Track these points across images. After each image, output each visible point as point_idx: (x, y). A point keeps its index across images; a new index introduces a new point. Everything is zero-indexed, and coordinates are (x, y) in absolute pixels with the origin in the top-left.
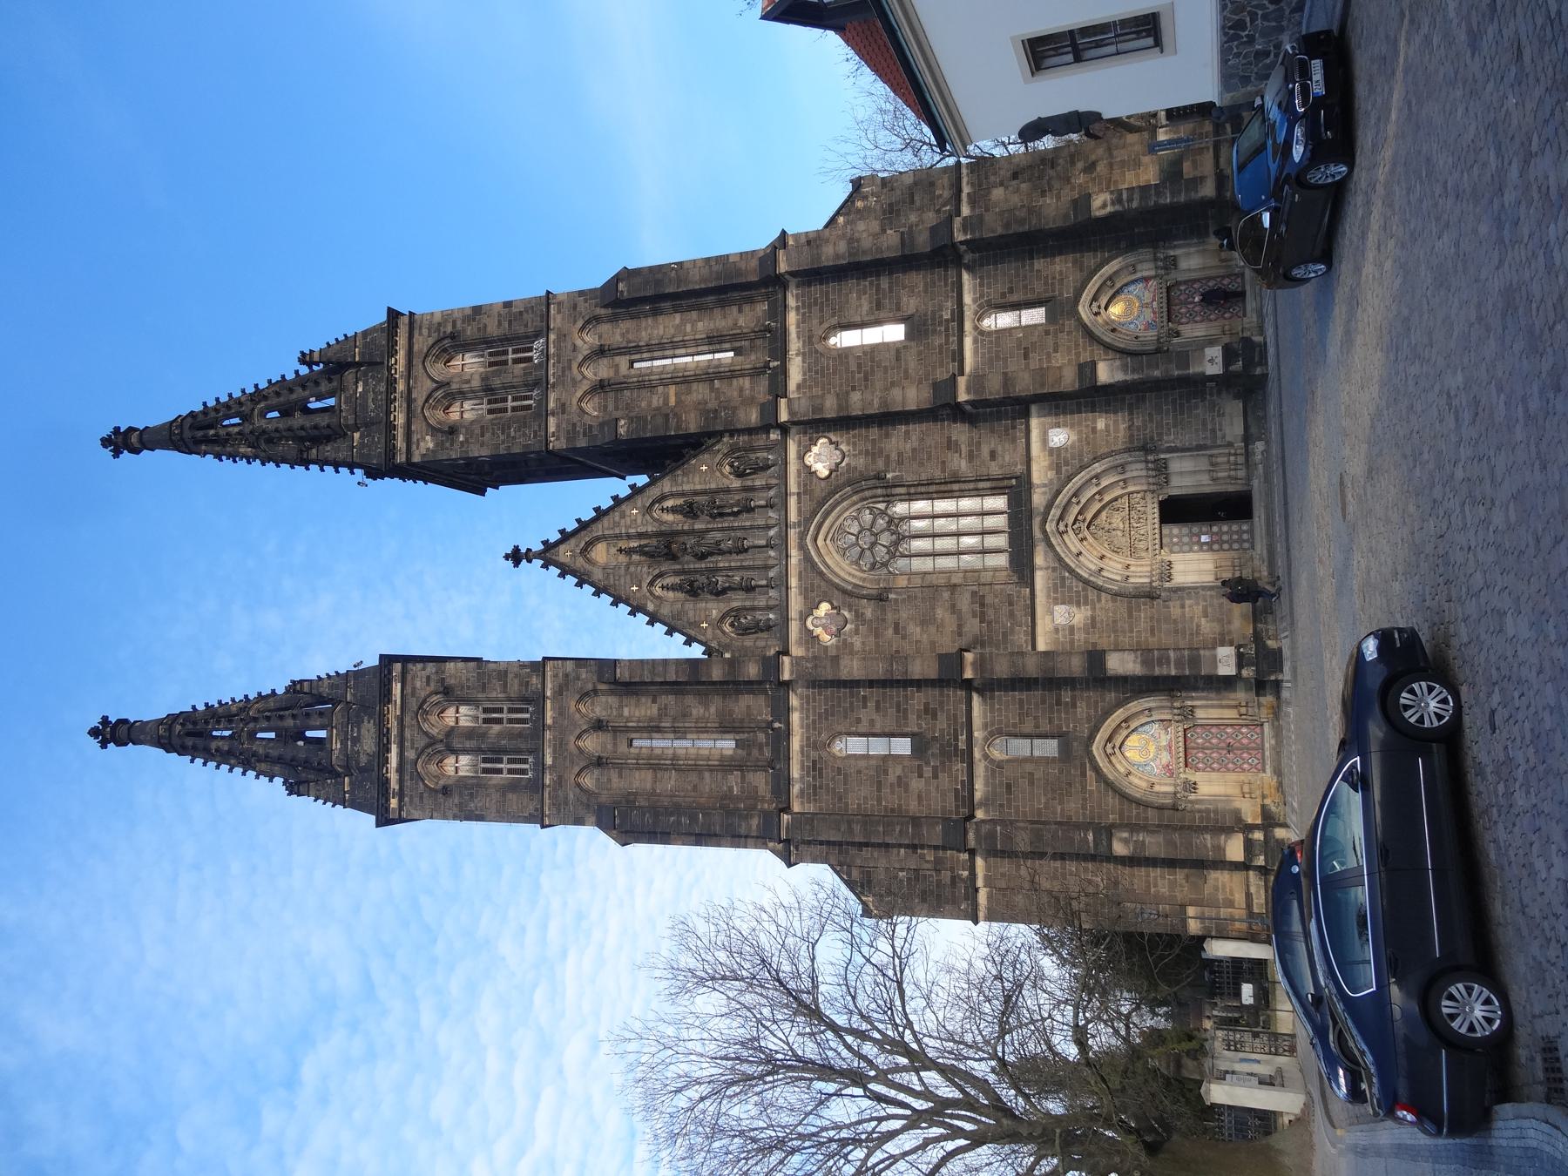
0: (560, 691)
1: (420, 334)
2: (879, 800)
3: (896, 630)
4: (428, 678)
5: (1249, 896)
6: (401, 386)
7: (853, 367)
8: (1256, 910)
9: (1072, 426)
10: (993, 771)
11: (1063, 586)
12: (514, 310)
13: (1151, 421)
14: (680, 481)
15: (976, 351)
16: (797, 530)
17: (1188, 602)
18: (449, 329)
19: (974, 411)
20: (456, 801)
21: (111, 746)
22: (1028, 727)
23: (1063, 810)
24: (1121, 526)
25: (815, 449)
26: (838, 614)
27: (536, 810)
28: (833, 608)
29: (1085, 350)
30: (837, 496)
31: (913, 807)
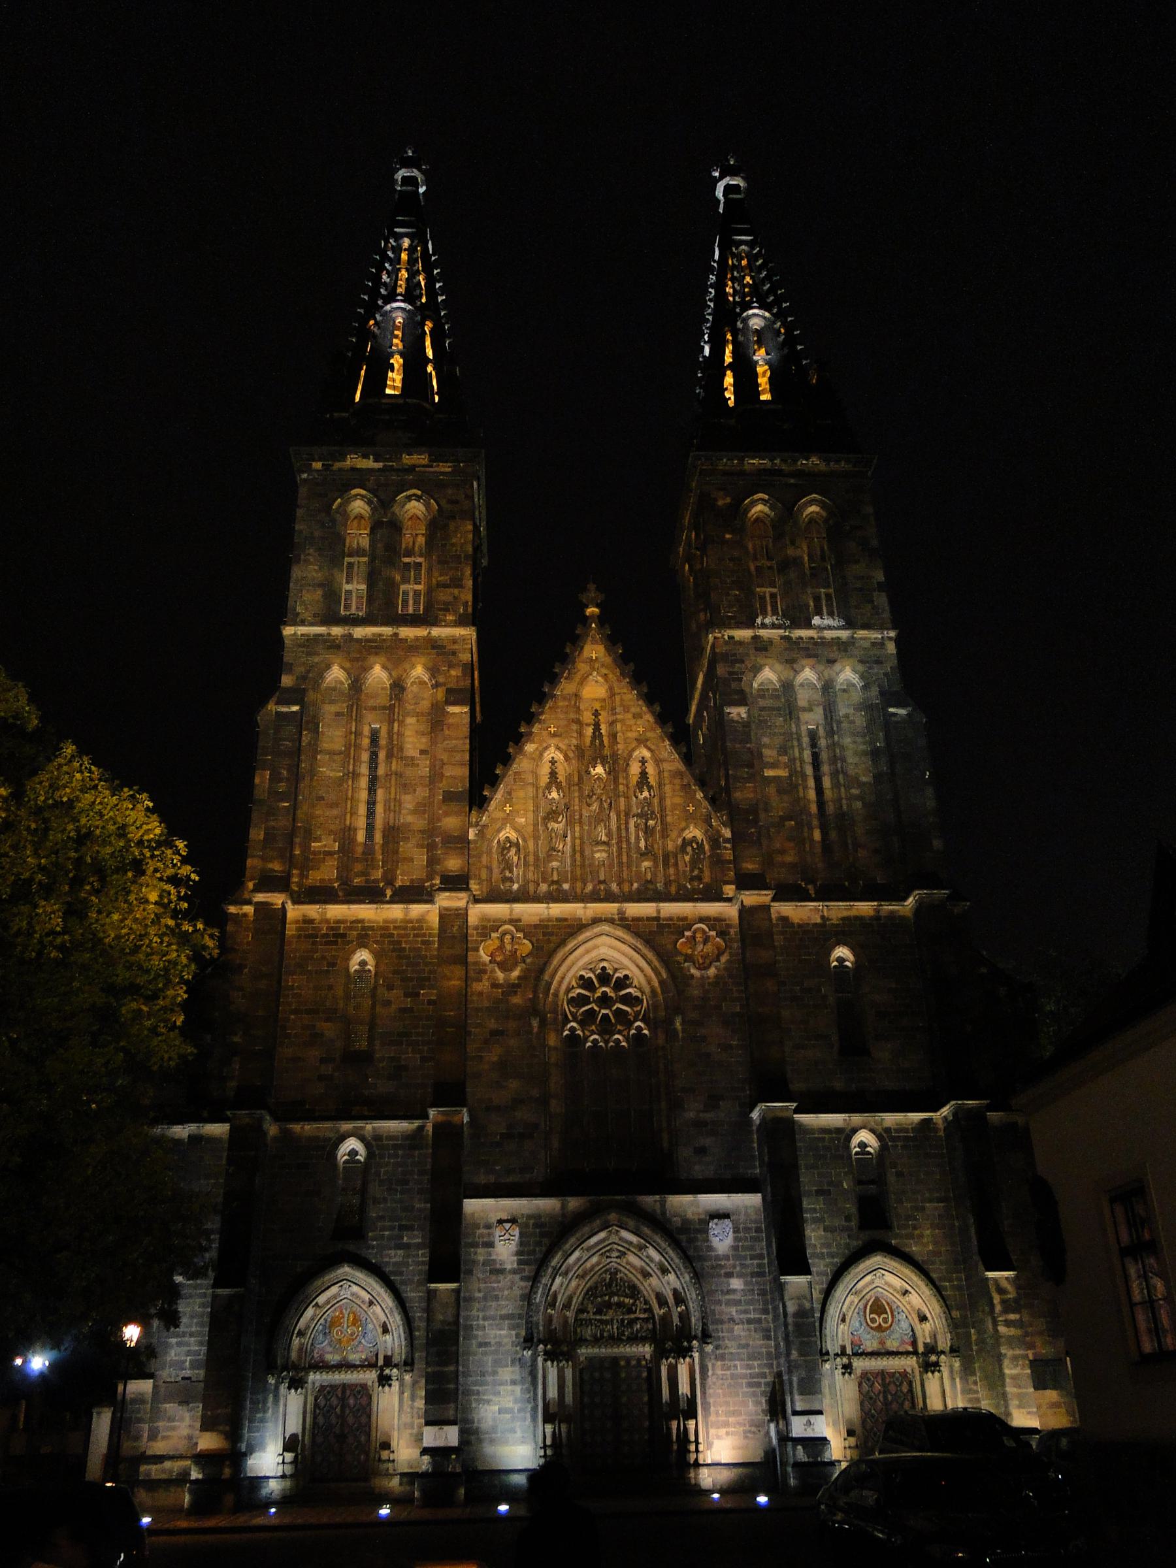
2: (295, 1012)
3: (495, 1033)
4: (457, 502)
5: (160, 1459)
8: (143, 1468)
9: (735, 1248)
13: (740, 1346)
15: (825, 1130)
16: (616, 917)
17: (518, 1389)
19: (755, 1128)
29: (826, 1266)
30: (656, 963)
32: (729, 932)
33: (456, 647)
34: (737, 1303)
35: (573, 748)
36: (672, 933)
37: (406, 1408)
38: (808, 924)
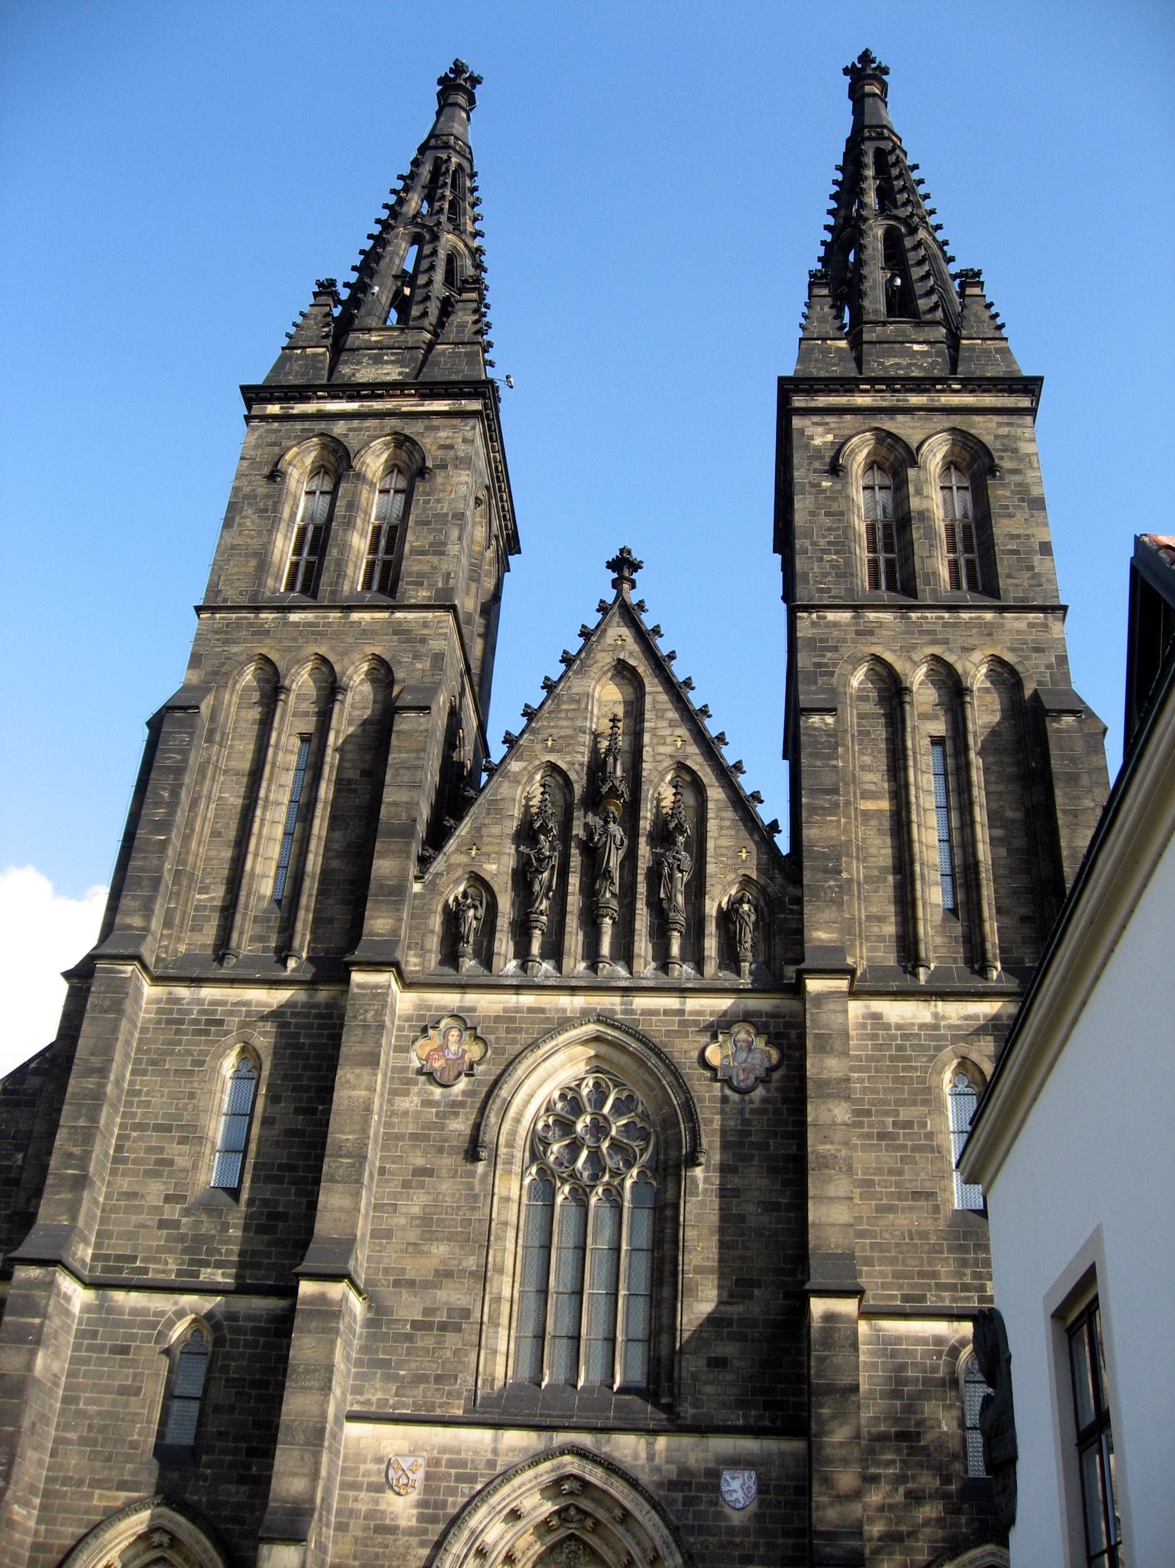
0: (400, 631)
1: (1000, 425)
4: (450, 447)
6: (915, 400)
7: (905, 1114)
9: (759, 1517)
10: (154, 1325)
11: (460, 1478)
14: (725, 814)
15: (923, 1340)
16: (618, 1008)
18: (1007, 464)
22: (221, 1395)
23: (68, 1442)
25: (760, 1043)
27: (225, 600)
32: (789, 1034)
33: (425, 632)
35: (577, 767)
38: (913, 1024)
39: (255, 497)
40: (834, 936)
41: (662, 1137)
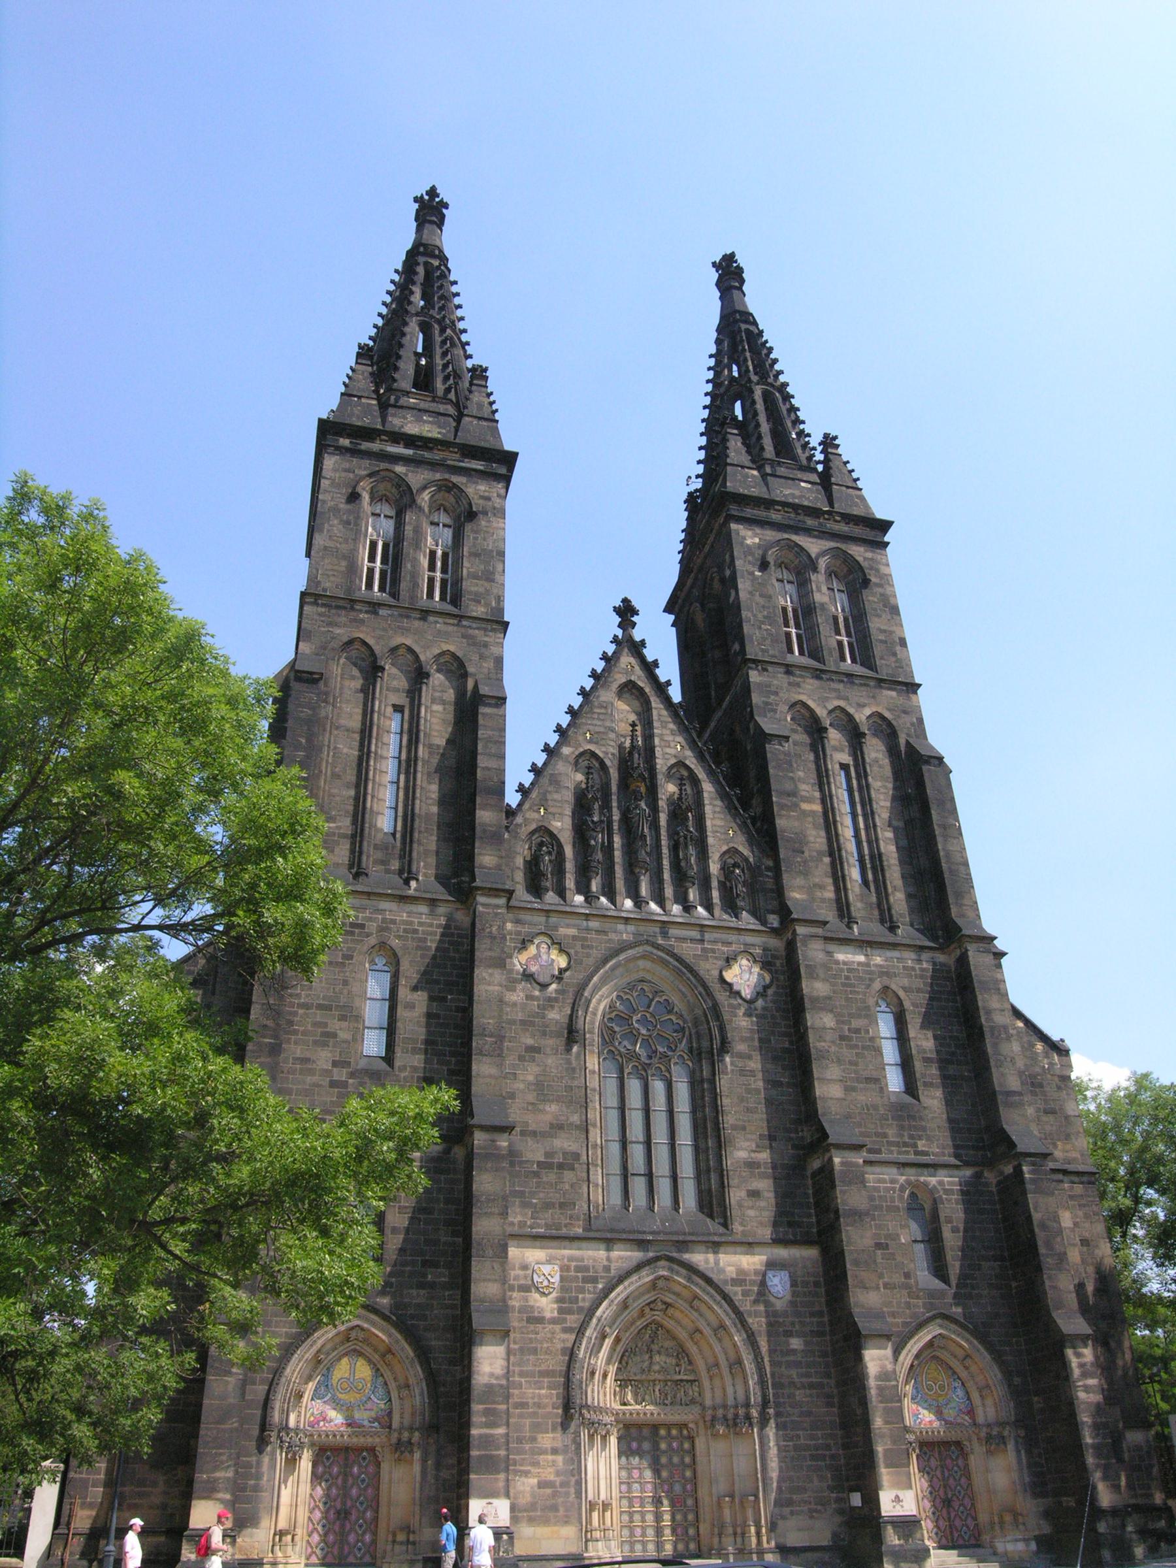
2: (306, 1006)
4: (488, 499)
6: (810, 522)
7: (855, 1023)
9: (792, 1303)
11: (586, 1280)
12: (898, 648)
17: (560, 1459)
18: (873, 579)
19: (809, 1173)
20: (342, 506)
21: (416, 206)
24: (656, 1368)
26: (553, 976)
27: (325, 590)
28: (561, 971)
31: (294, 1049)
34: (797, 1364)
36: (716, 958)
37: (430, 1479)
39: (339, 510)
40: (804, 897)
41: (693, 1031)
